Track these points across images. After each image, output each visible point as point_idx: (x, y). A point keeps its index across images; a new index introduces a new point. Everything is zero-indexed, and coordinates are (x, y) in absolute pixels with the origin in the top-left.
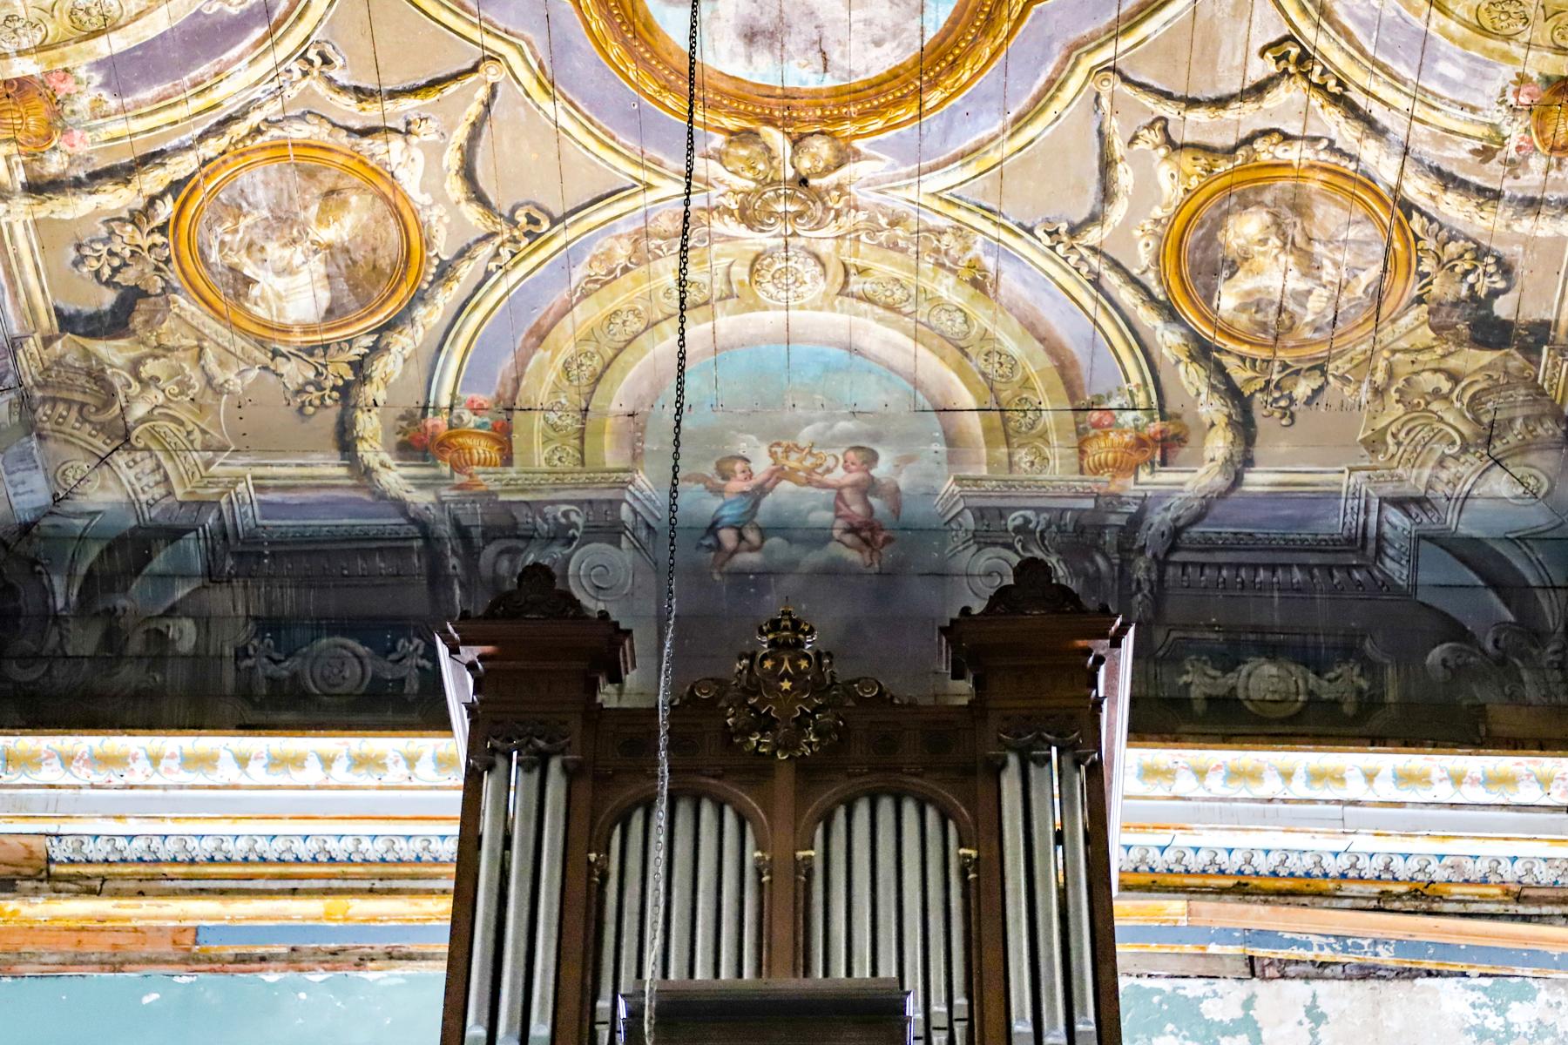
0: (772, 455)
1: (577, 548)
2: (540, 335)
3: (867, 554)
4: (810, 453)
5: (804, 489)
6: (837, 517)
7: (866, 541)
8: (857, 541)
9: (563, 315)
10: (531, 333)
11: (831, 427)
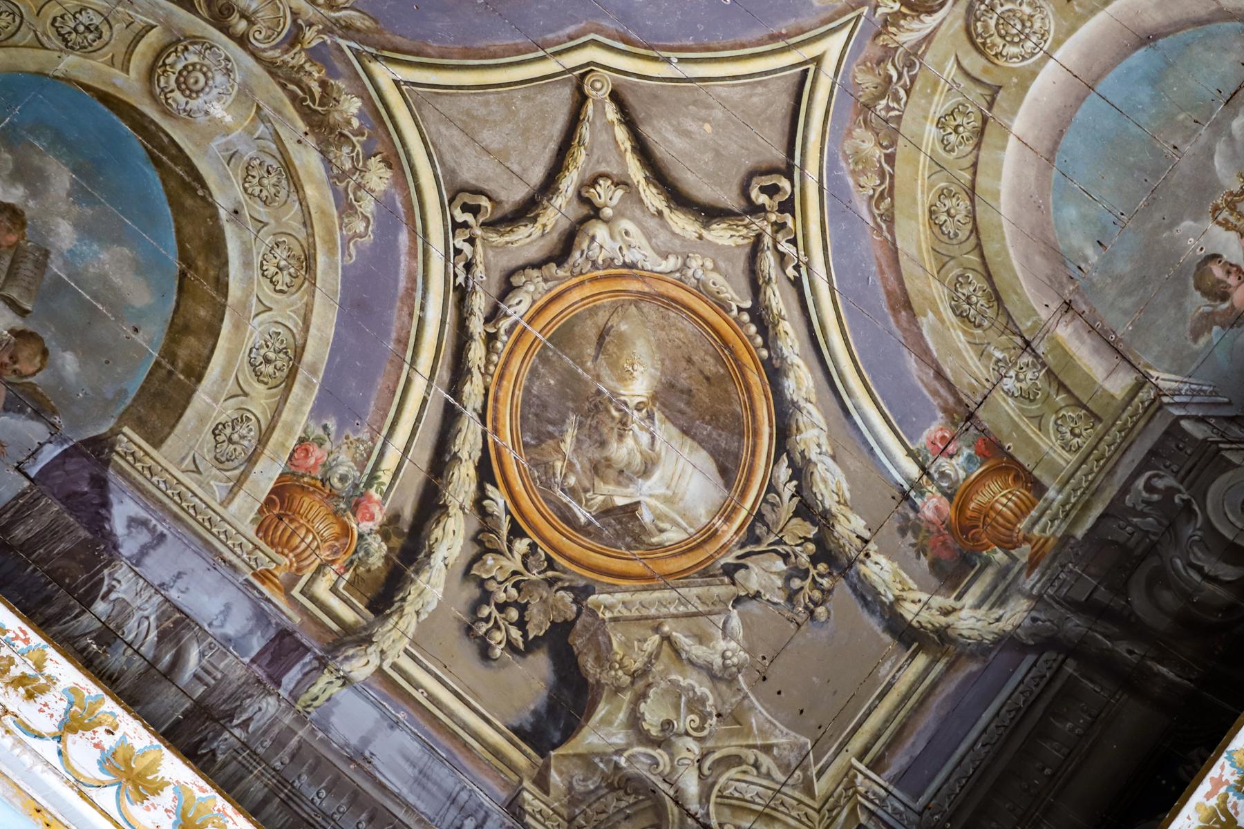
2: (902, 303)
9: (896, 260)
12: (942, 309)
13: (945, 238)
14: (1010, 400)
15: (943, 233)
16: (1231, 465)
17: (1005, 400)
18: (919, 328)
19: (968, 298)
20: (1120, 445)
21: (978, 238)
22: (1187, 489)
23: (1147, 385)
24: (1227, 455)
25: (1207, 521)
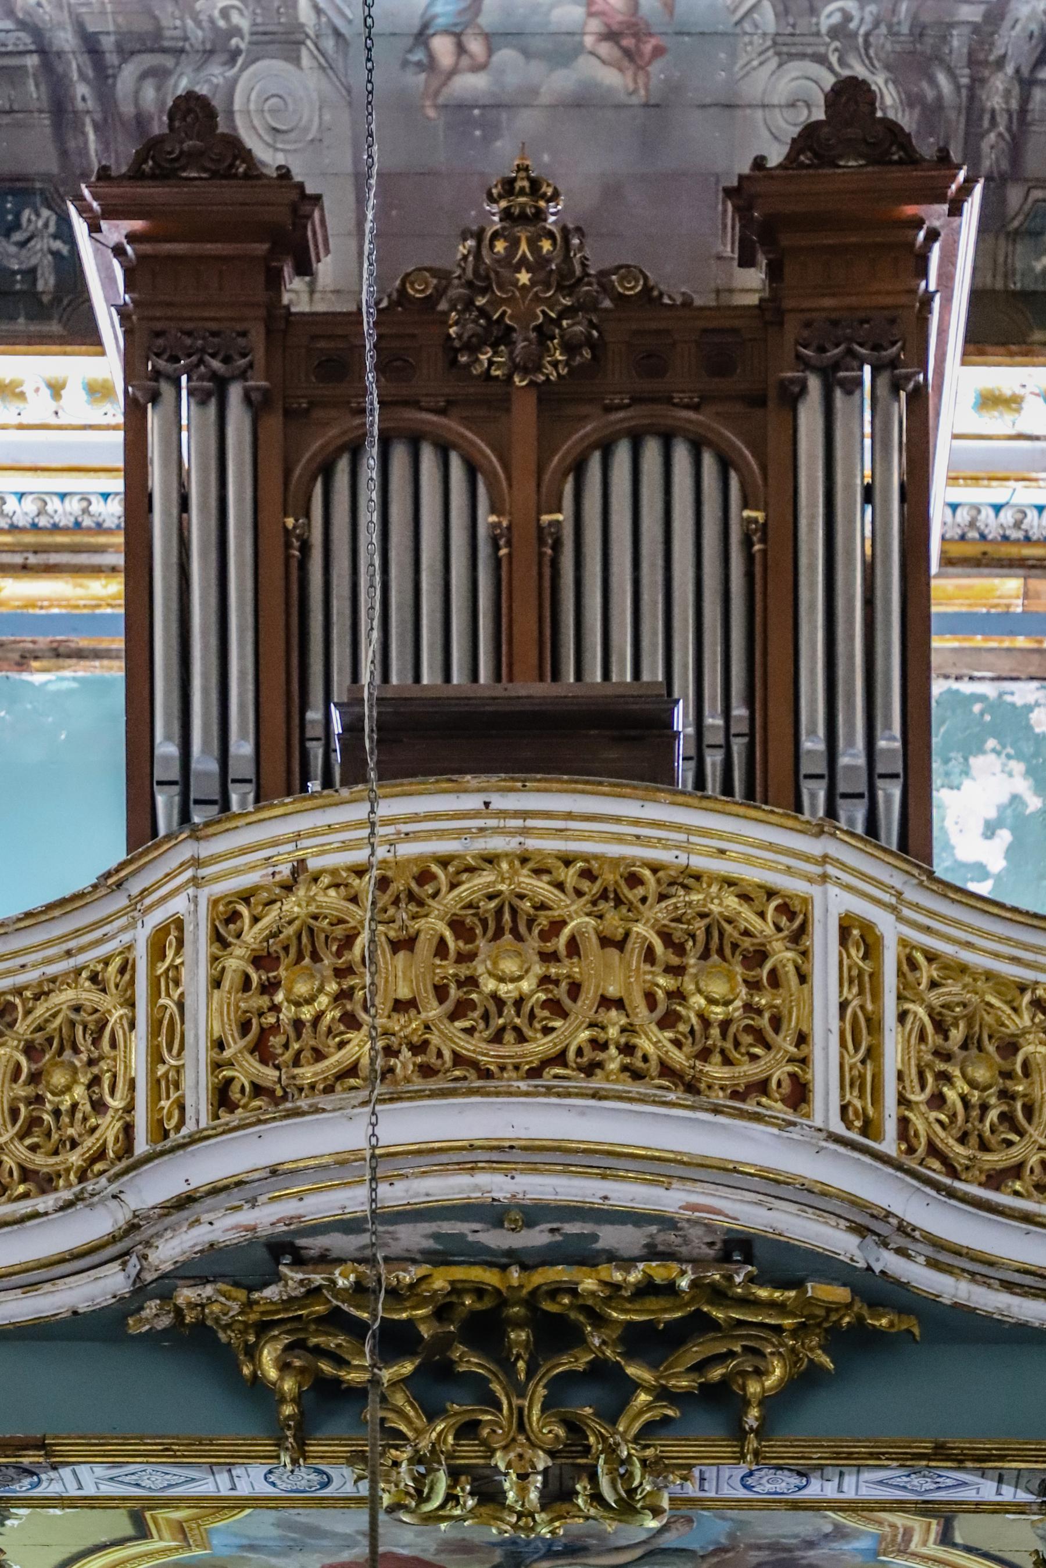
1: (242, 70)
3: (630, 73)
7: (627, 53)
8: (617, 53)
16: (297, 61)
22: (251, 43)
24: (304, 53)
25: (235, 81)
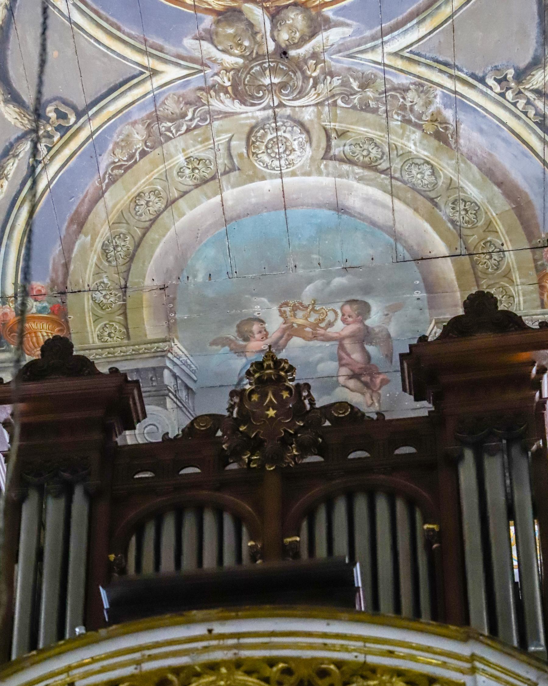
0: (282, 314)
2: (80, 222)
4: (313, 309)
5: (311, 343)
6: (341, 365)
10: (72, 221)
11: (329, 283)
12: (97, 240)
13: (133, 212)
14: (91, 301)
15: (135, 209)
17: (88, 299)
18: (77, 239)
19: (117, 246)
20: (127, 355)
21: (151, 226)
23: (168, 343)
